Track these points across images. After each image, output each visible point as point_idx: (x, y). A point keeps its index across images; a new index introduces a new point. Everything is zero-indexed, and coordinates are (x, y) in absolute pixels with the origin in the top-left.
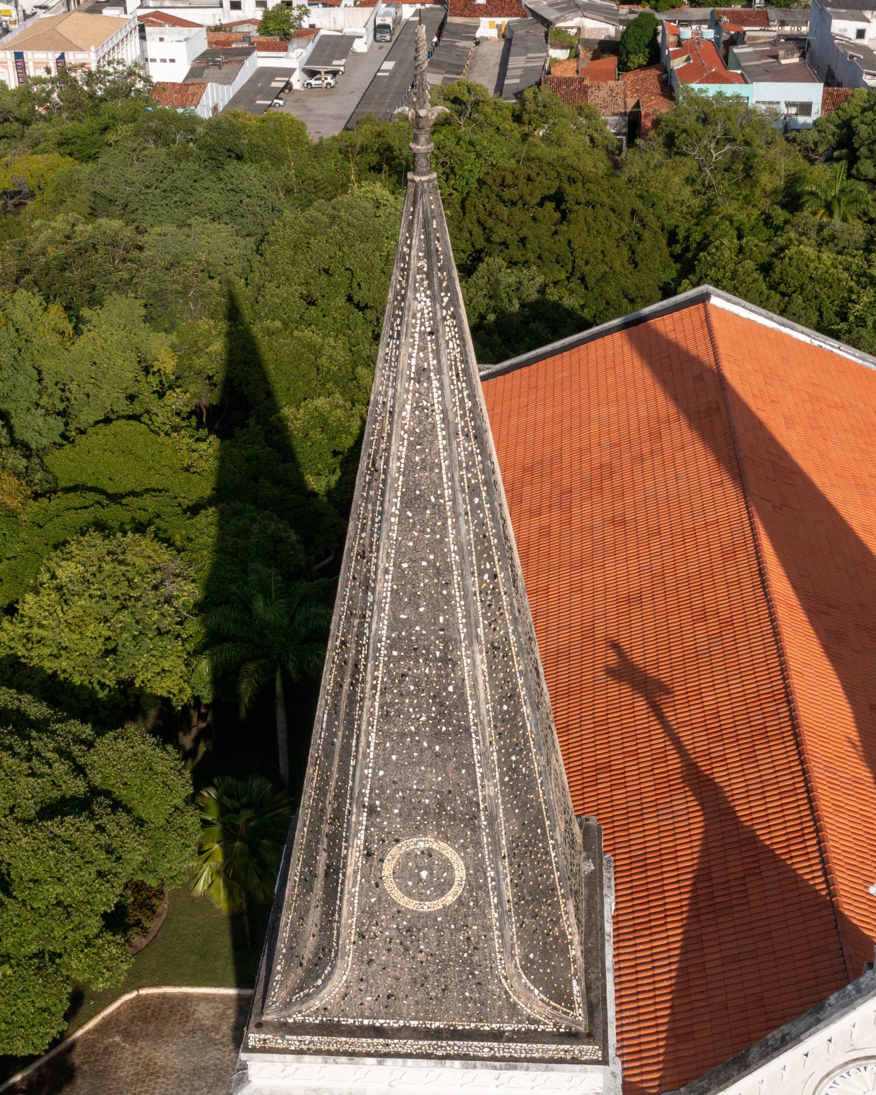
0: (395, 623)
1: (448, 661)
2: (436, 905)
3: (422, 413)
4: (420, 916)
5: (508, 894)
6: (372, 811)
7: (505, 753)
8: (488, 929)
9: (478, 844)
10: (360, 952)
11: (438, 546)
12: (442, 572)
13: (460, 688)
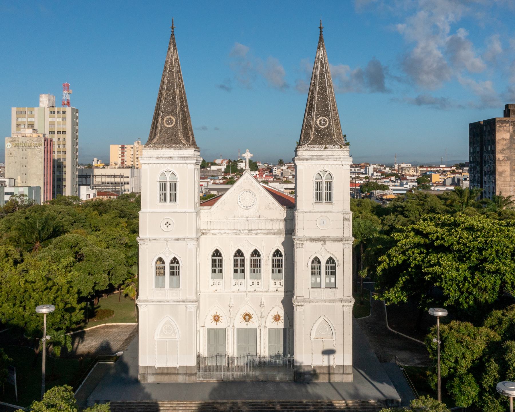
0: (167, 86)
1: (174, 91)
2: (171, 126)
3: (171, 61)
4: (168, 128)
5: (181, 125)
6: (163, 112)
7: (181, 106)
8: (178, 129)
9: (177, 117)
10: (160, 134)
11: (173, 76)
12: (173, 79)
13: (175, 95)
